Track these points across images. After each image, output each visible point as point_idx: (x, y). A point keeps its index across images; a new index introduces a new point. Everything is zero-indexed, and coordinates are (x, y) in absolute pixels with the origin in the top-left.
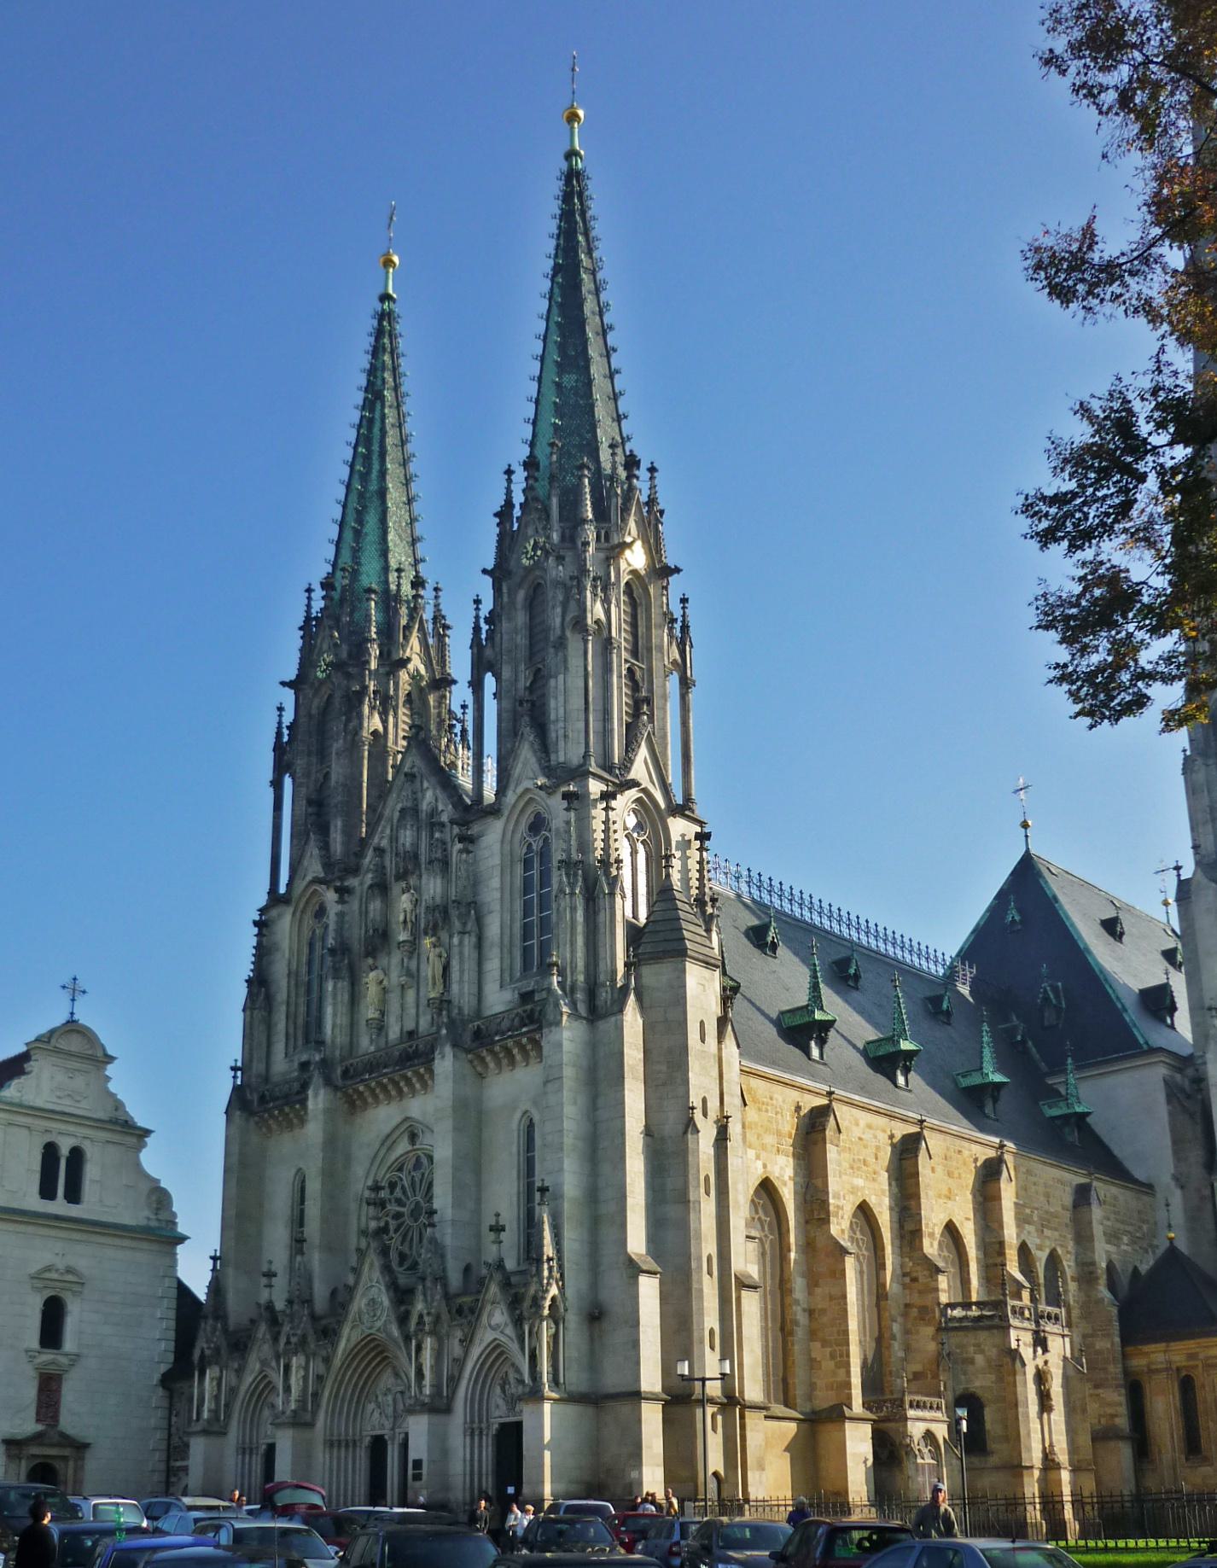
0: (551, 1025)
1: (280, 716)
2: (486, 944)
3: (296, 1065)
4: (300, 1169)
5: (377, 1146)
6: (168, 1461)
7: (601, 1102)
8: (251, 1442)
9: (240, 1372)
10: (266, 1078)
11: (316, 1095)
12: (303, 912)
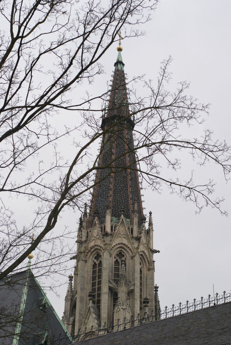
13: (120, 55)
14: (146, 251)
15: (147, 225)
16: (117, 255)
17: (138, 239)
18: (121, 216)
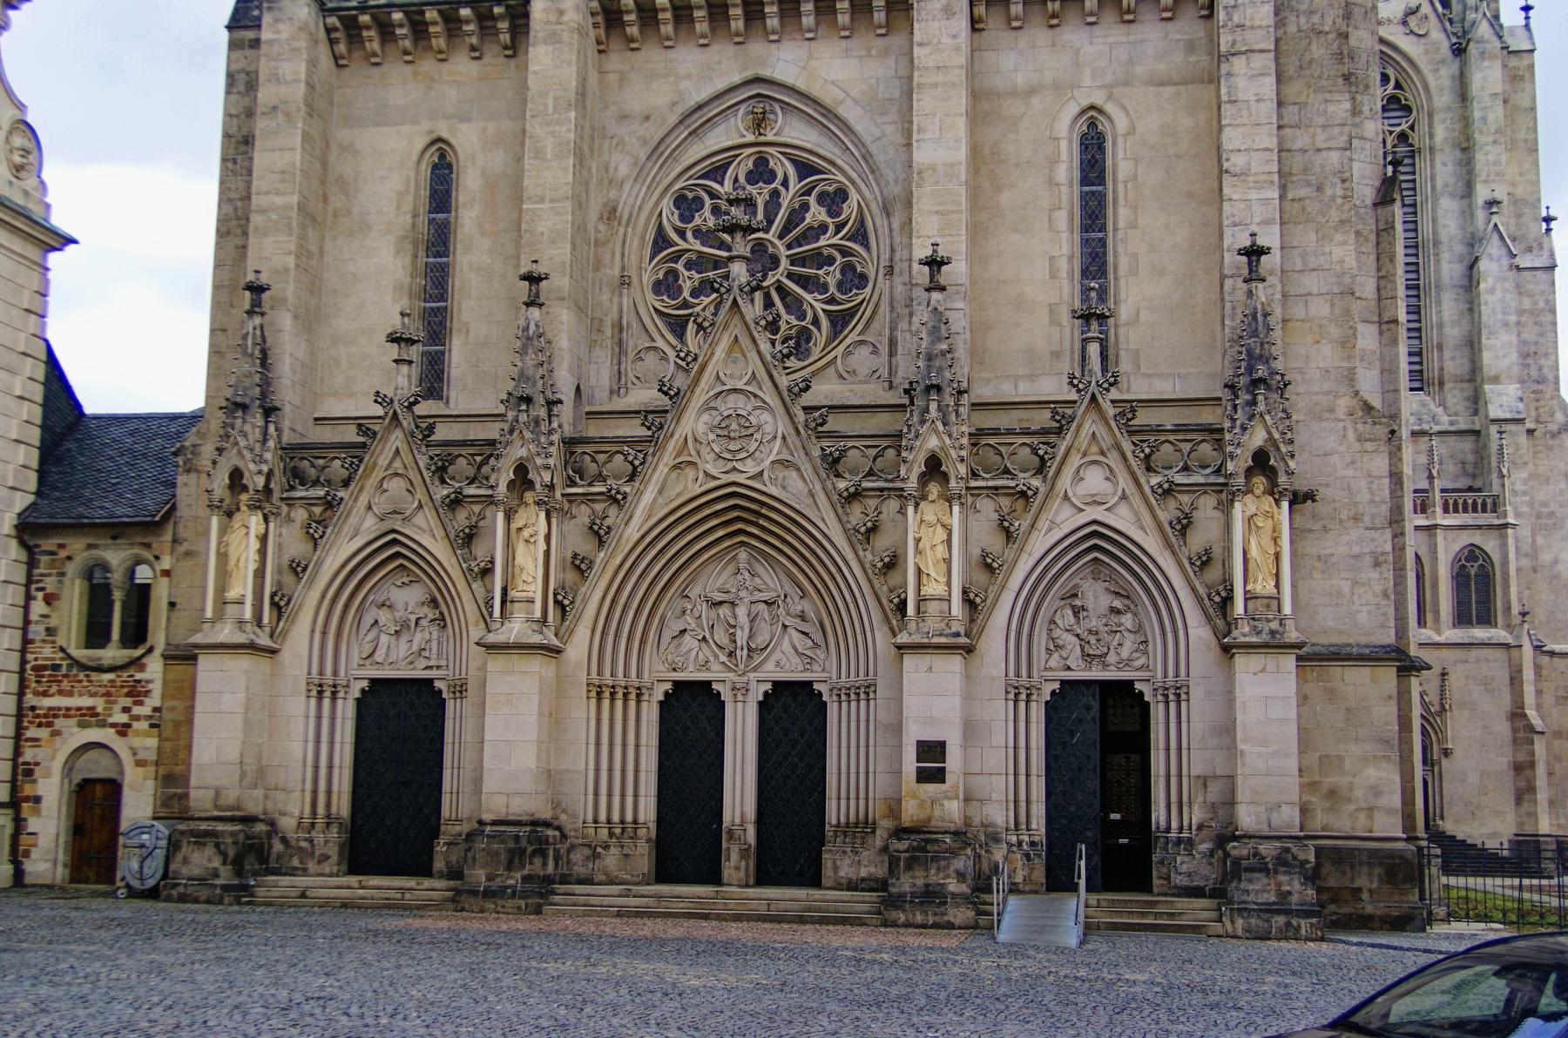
4: (440, 140)
5: (673, 119)
6: (21, 694)
8: (335, 673)
9: (316, 534)
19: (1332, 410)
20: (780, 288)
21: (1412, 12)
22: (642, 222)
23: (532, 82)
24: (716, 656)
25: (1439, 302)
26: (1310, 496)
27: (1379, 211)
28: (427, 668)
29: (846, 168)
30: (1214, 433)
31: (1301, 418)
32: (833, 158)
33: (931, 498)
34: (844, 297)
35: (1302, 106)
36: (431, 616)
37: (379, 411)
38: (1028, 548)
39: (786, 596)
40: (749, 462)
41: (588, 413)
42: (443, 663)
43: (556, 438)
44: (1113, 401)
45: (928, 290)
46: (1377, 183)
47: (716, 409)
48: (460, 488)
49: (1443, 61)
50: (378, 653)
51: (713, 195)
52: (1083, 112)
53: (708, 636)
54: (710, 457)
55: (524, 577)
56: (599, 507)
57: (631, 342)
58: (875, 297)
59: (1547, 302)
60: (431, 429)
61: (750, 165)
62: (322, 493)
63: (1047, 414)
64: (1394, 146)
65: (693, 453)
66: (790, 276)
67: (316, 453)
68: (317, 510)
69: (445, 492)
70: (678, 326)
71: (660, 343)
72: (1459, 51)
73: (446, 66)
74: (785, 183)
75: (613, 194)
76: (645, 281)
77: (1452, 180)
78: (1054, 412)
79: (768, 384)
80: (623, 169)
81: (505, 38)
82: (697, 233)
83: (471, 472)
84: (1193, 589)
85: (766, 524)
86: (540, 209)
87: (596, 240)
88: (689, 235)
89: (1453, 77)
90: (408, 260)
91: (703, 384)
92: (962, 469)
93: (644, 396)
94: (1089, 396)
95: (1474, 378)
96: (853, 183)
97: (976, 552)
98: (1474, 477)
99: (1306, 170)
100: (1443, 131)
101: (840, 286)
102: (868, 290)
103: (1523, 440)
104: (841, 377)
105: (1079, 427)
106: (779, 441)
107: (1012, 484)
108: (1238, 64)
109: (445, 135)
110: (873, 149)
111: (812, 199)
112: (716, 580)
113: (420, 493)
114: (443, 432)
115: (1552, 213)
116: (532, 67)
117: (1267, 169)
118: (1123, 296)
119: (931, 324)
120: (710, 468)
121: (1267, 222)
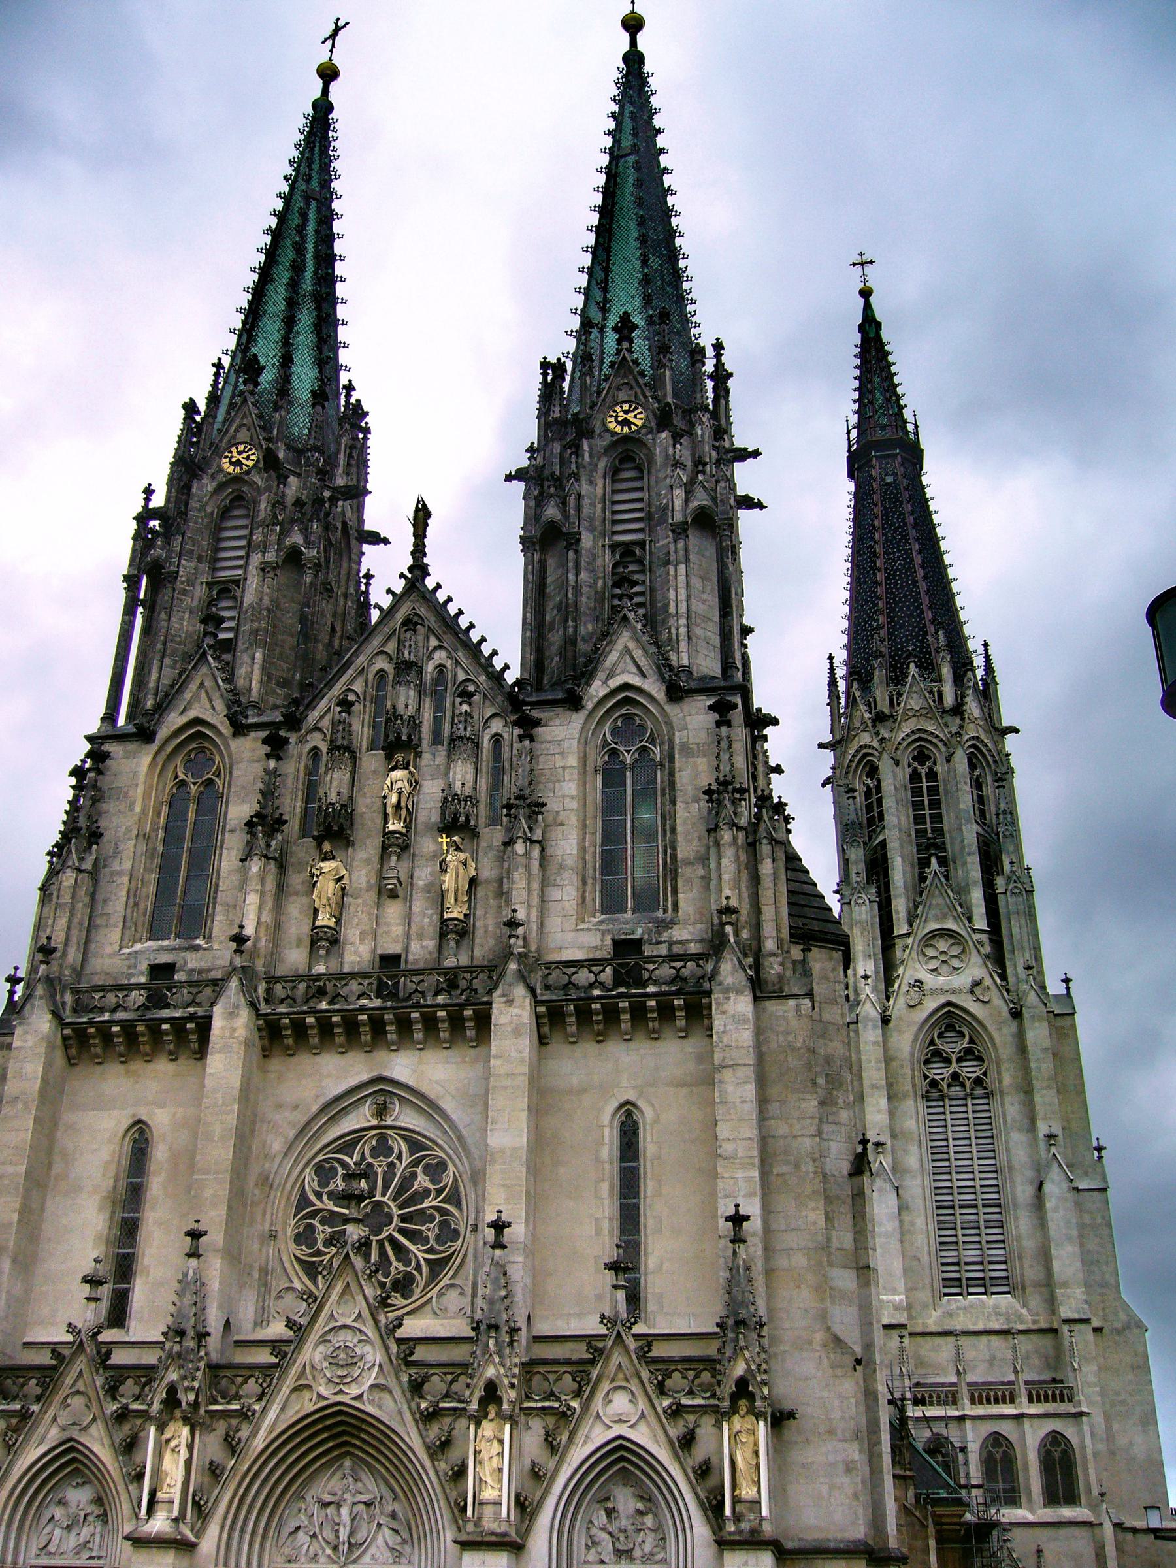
0: (727, 990)
1: (147, 500)
2: (552, 869)
3: (144, 966)
4: (140, 1121)
5: (315, 1108)
7: (773, 1108)
10: (78, 972)
11: (232, 1015)
12: (170, 757)
13: (867, 307)
14: (983, 737)
15: (980, 673)
16: (914, 759)
17: (958, 710)
18: (908, 667)
19: (810, 1342)
20: (391, 1239)
21: (976, 984)
22: (289, 1186)
23: (208, 1081)
24: (324, 1551)
25: (1016, 1219)
26: (791, 1415)
27: (854, 1179)
28: (90, 1558)
29: (445, 1146)
30: (708, 1362)
31: (786, 1348)
32: (436, 1138)
33: (490, 1417)
34: (440, 1248)
35: (783, 1102)
36: (97, 1512)
37: (69, 1338)
38: (568, 1459)
39: (381, 1498)
40: (353, 1385)
41: (236, 1342)
42: (104, 1554)
43: (202, 1364)
44: (634, 1336)
45: (493, 1247)
46: (851, 1158)
47: (329, 1341)
48: (127, 1404)
49: (1004, 1022)
50: (50, 1547)
51: (344, 1165)
52: (622, 1106)
53: (317, 1531)
54: (323, 1381)
55: (168, 1481)
56: (234, 1422)
57: (274, 1284)
58: (464, 1249)
59: (1103, 1217)
60: (108, 1355)
61: (374, 1143)
62: (18, 1407)
63: (583, 1347)
64: (972, 1089)
65: (310, 1377)
66: (401, 1231)
67: (19, 1373)
68: (14, 1421)
69: (115, 1408)
70: (311, 1270)
71: (297, 1285)
72: (1016, 1014)
73: (151, 1066)
74: (400, 1158)
75: (267, 1165)
76: (289, 1234)
77: (1018, 1117)
78: (589, 1345)
79: (370, 1322)
80: (277, 1145)
81: (195, 1045)
82: (331, 1195)
83: (137, 1390)
84: (696, 1494)
85: (366, 1437)
86: (206, 1180)
87: (252, 1202)
88: (325, 1197)
89: (1013, 1036)
90: (108, 1215)
91: (321, 1321)
92: (513, 1394)
93: (277, 1329)
94: (615, 1333)
95: (1048, 1284)
96: (450, 1158)
97: (527, 1463)
98: (1056, 1369)
99: (786, 1152)
100: (1007, 1080)
101: (438, 1238)
102: (459, 1242)
103: (1090, 1336)
104: (435, 1313)
105: (608, 1358)
106: (376, 1369)
107: (556, 1405)
108: (727, 1075)
109: (144, 1118)
110: (464, 1132)
111: (419, 1170)
112: (328, 1485)
113: (95, 1408)
114: (119, 1357)
115: (1102, 1143)
116: (209, 1070)
117: (749, 1154)
118: (650, 1250)
119: (492, 1276)
120: (323, 1391)
121: (751, 1194)
